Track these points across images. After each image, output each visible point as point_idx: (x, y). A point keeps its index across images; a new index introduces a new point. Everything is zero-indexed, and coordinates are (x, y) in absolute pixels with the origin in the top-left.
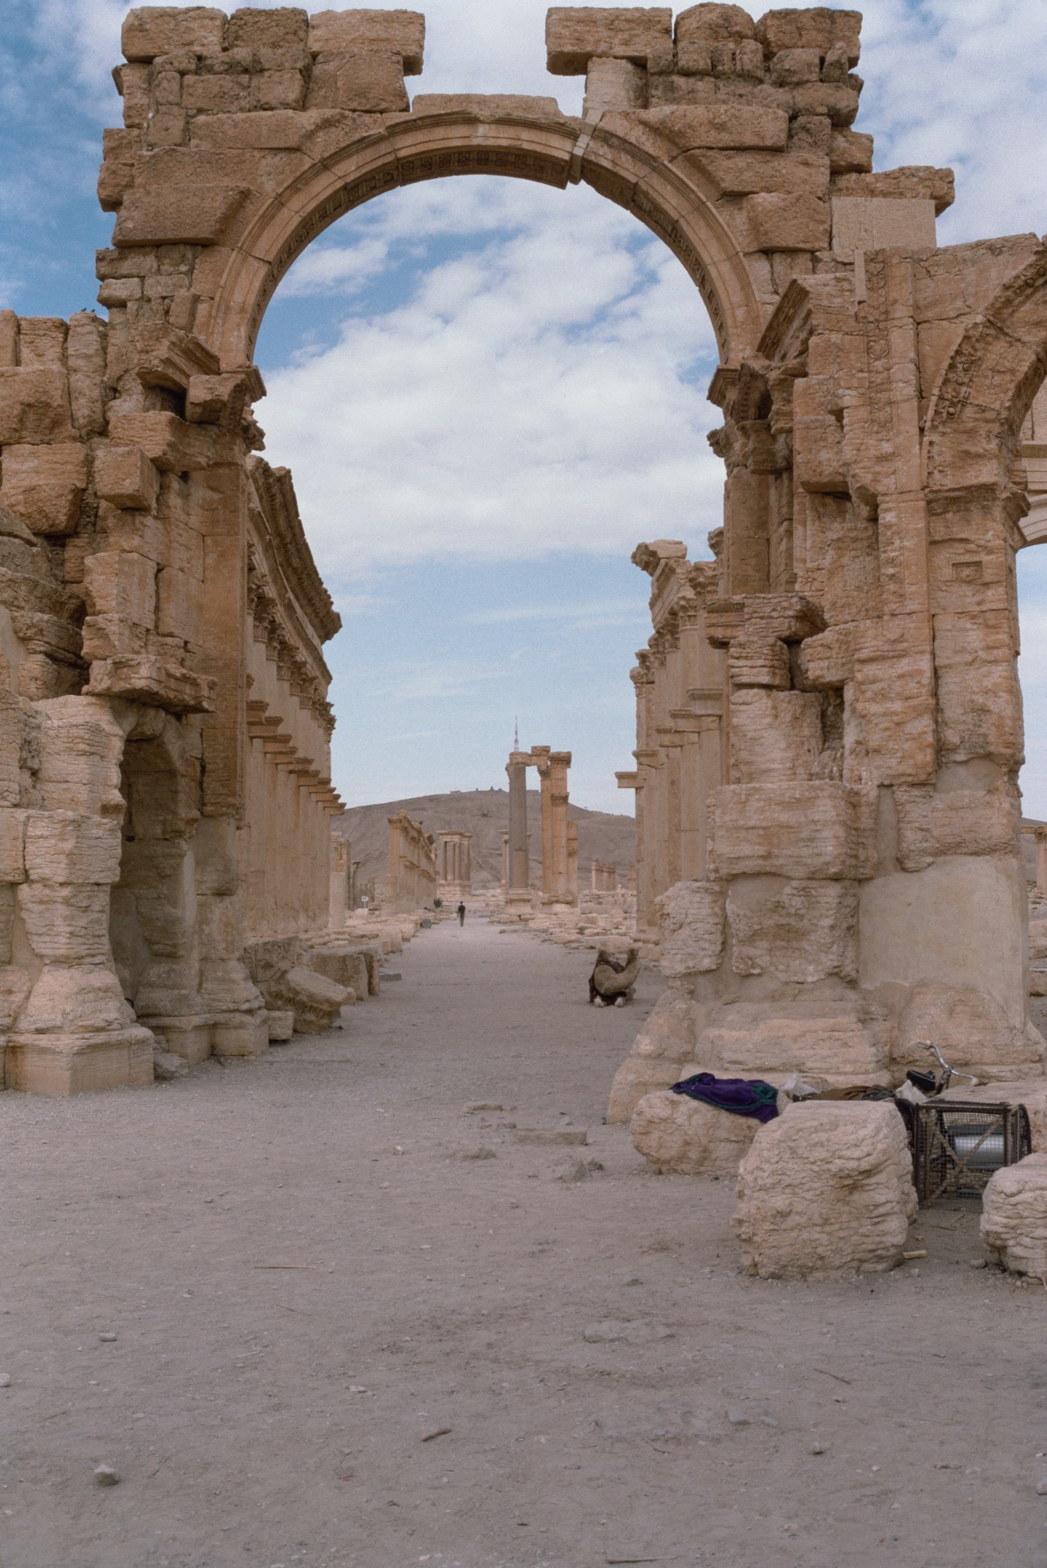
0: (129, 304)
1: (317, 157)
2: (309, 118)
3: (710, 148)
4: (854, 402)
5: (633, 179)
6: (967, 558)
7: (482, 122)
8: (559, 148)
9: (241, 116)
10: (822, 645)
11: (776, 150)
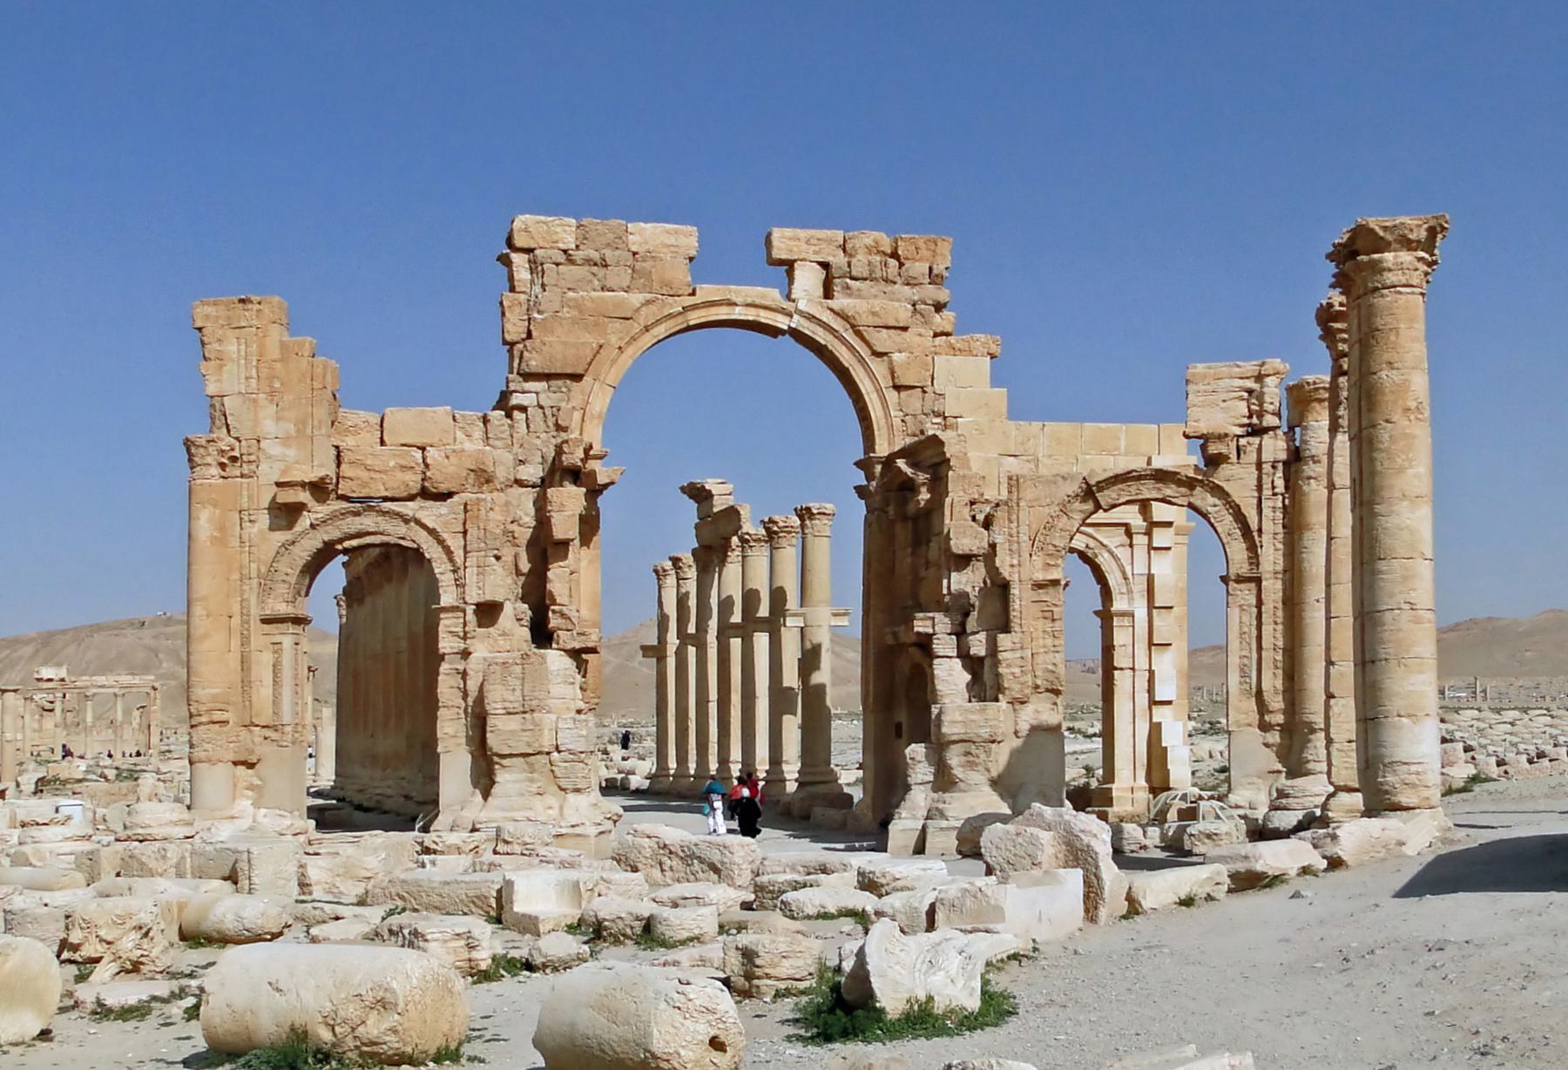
1: (643, 324)
2: (636, 298)
5: (823, 342)
6: (1046, 609)
8: (782, 322)
9: (594, 294)
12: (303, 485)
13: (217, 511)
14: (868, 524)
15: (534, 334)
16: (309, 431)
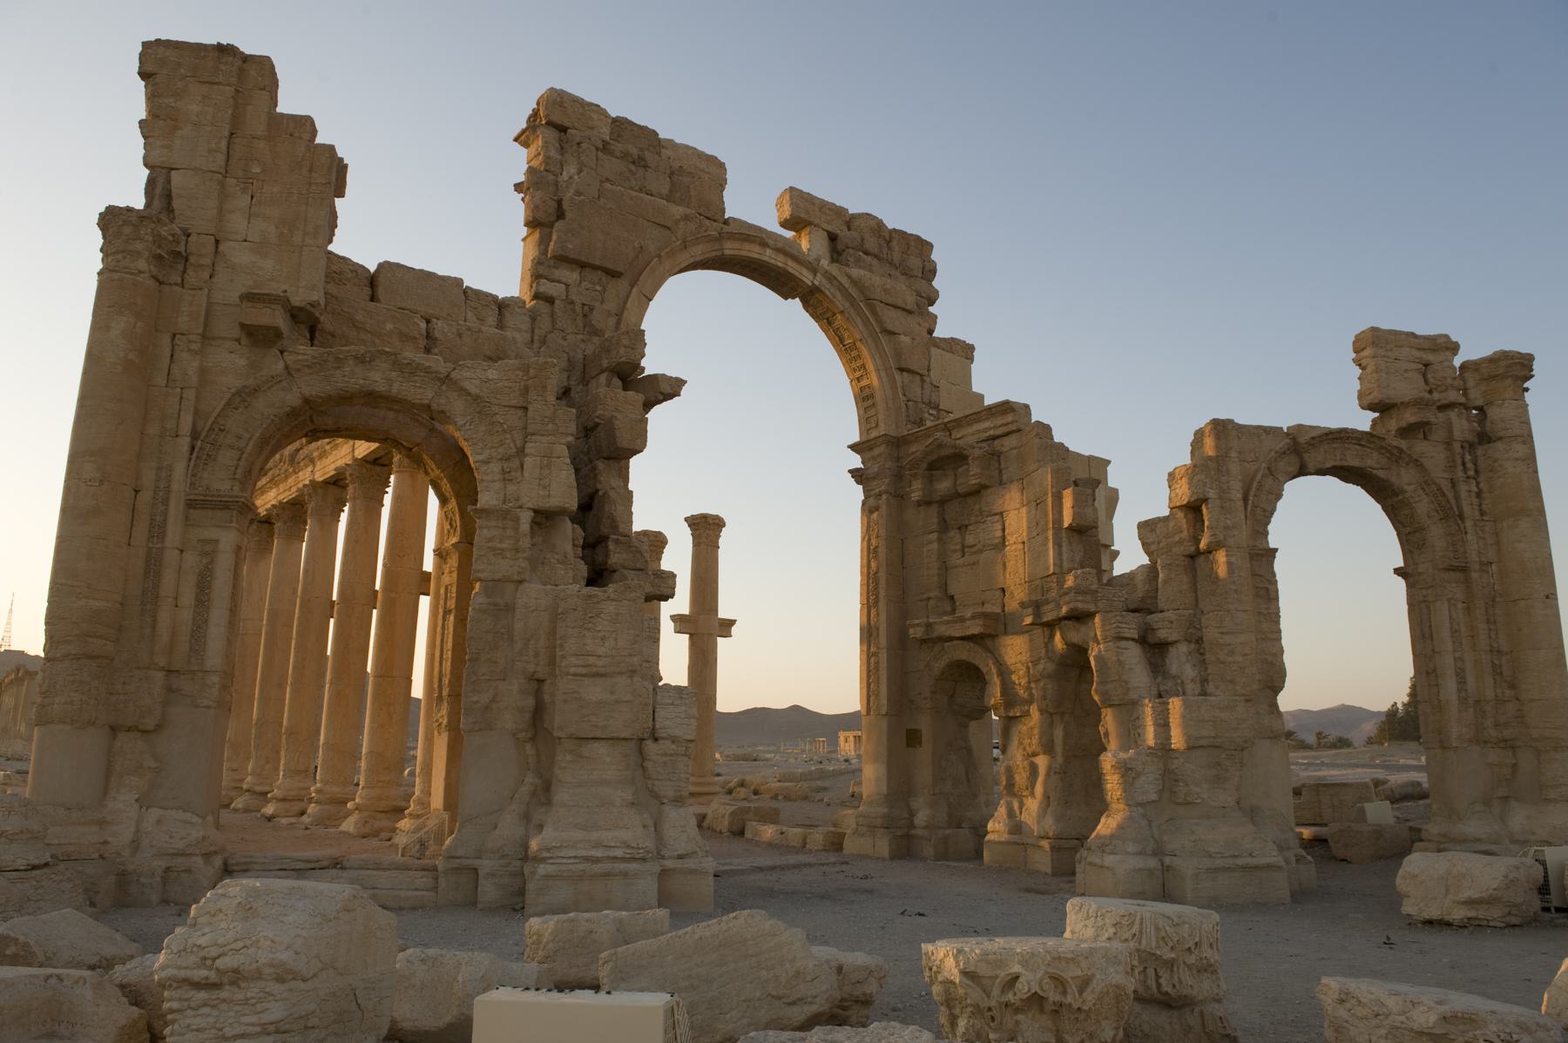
0: (557, 302)
2: (677, 211)
3: (882, 302)
4: (1215, 496)
7: (769, 247)
10: (1168, 621)
11: (910, 312)
12: (283, 302)
13: (139, 324)
14: (868, 509)
15: (569, 215)
16: (297, 239)
